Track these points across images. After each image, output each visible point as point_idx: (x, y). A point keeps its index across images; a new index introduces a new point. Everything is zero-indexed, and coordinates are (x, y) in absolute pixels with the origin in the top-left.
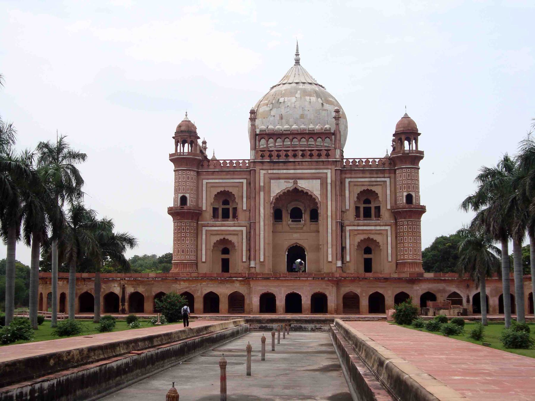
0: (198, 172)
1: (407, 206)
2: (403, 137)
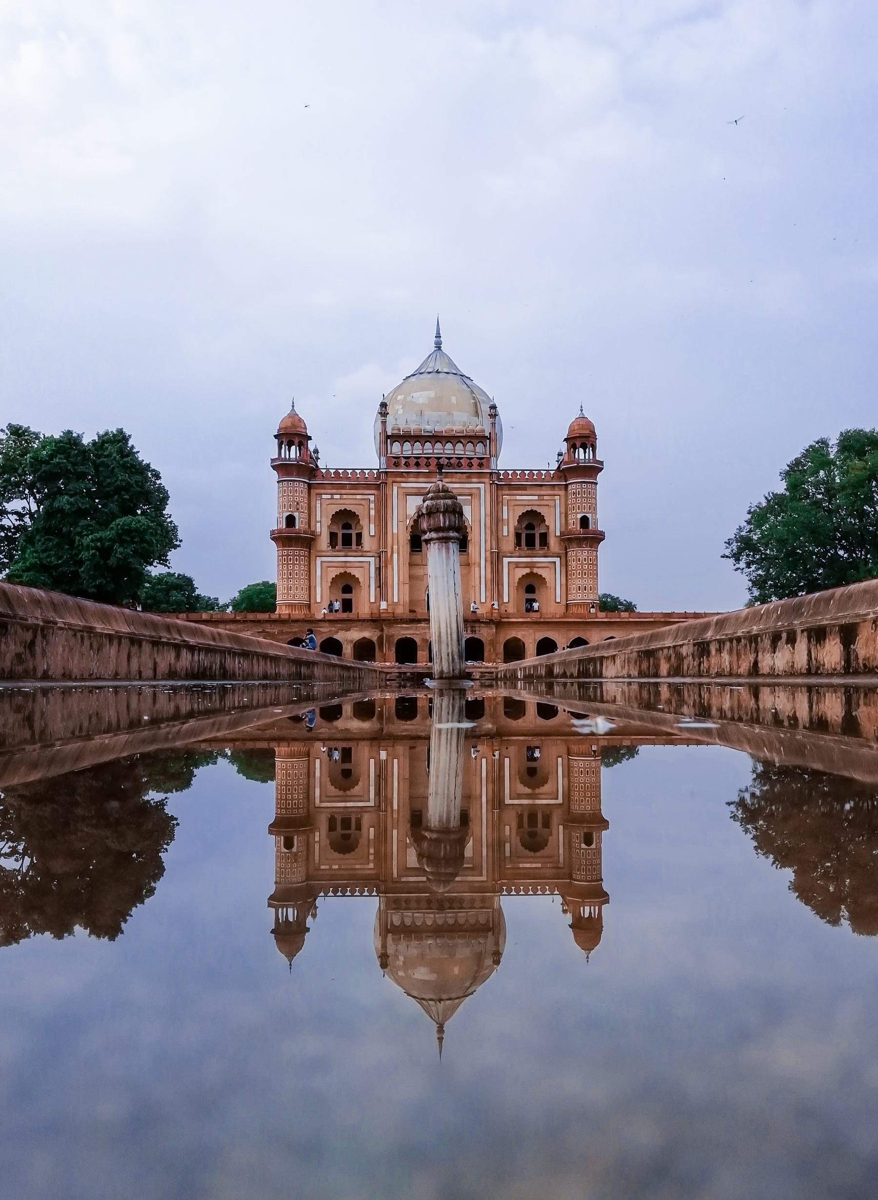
0: (310, 486)
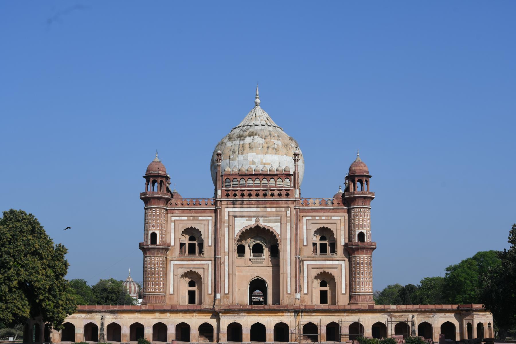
1: (360, 243)
2: (357, 179)
